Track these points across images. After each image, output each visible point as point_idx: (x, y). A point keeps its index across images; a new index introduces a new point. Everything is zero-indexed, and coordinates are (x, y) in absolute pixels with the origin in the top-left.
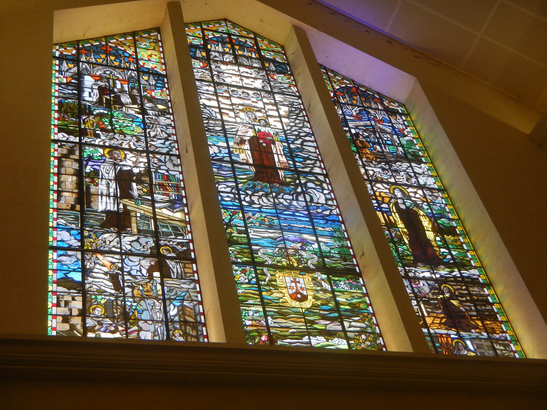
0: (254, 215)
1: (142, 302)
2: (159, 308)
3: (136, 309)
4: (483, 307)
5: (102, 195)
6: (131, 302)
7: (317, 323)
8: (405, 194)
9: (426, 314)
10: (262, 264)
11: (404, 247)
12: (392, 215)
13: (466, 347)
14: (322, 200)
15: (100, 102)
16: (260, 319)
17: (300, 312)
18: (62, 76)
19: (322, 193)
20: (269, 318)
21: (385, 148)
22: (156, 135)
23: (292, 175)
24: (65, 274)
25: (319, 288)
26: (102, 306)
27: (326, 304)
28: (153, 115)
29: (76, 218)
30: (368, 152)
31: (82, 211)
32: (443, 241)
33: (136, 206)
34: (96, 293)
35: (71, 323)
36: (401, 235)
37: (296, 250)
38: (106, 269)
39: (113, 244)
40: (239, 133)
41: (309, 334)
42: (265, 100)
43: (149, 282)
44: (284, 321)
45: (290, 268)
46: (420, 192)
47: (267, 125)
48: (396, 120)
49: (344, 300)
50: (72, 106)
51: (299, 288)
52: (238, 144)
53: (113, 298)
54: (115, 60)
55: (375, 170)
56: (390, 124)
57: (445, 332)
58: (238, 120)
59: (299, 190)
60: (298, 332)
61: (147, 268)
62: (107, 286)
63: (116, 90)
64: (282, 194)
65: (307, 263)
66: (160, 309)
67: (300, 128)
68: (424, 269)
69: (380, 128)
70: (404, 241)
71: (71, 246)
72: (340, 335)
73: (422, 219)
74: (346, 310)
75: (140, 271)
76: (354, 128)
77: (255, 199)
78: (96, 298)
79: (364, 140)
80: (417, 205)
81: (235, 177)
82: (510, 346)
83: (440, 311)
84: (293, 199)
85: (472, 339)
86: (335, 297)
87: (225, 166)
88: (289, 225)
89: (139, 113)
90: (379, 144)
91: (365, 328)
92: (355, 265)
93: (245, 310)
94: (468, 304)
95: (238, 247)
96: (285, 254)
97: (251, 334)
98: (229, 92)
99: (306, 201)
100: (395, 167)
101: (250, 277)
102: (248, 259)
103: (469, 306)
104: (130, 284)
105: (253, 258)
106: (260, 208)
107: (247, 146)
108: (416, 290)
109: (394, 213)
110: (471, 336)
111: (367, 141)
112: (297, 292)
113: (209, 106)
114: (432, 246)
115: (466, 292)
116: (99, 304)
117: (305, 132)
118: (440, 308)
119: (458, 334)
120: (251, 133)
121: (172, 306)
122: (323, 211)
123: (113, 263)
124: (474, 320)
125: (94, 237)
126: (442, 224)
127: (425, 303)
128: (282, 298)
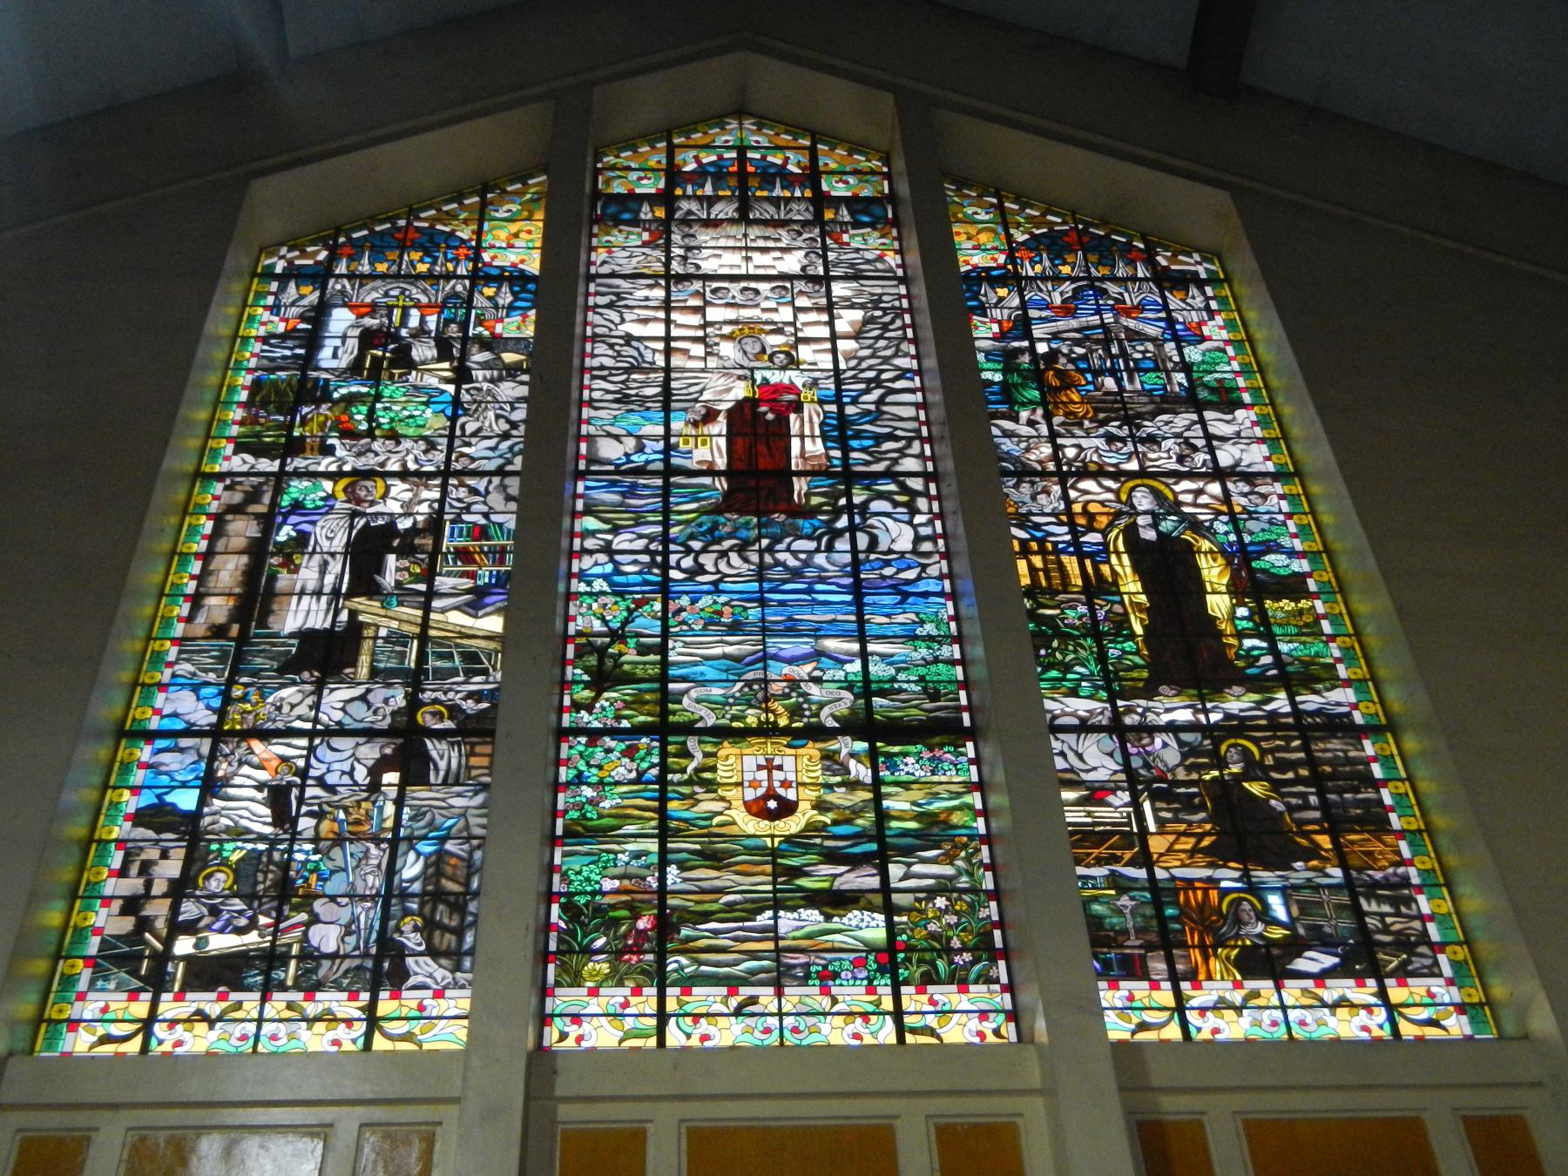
0: (694, 602)
1: (336, 853)
2: (376, 862)
3: (316, 870)
4: (1348, 796)
5: (302, 593)
6: (307, 853)
7: (808, 874)
8: (1166, 498)
9: (1152, 827)
10: (689, 729)
11: (1129, 645)
12: (1108, 562)
13: (1265, 915)
14: (905, 543)
15: (355, 369)
16: (644, 872)
17: (766, 848)
18: (276, 319)
19: (910, 523)
20: (672, 870)
21: (1131, 380)
22: (480, 429)
23: (829, 486)
24: (159, 797)
25: (838, 779)
26: (230, 867)
27: (848, 821)
28: (485, 379)
29: (221, 659)
30: (1075, 397)
31: (243, 639)
32: (1257, 618)
33: (382, 612)
34: (225, 836)
35: (144, 913)
36: (1126, 614)
37: (794, 683)
38: (263, 776)
39: (298, 711)
40: (706, 396)
41: (777, 905)
42: (802, 302)
43: (366, 799)
44: (713, 873)
45: (766, 731)
46: (1215, 488)
47: (792, 362)
48: (1183, 301)
49: (907, 806)
50: (283, 386)
51: (776, 784)
52: (695, 424)
53: (262, 847)
54: (421, 261)
55: (1085, 443)
56: (1163, 315)
57: (1207, 873)
58: (712, 363)
59: (843, 522)
60: (746, 901)
61: (370, 763)
62: (255, 815)
63: (404, 332)
64: (788, 540)
65: (817, 715)
66: (379, 866)
67: (886, 360)
68: (1176, 702)
69: (1127, 329)
70: (1130, 628)
71: (194, 724)
72: (870, 903)
73: (1203, 562)
74: (905, 833)
75: (351, 773)
76: (1048, 341)
77: (707, 561)
78: (220, 851)
79: (1070, 366)
80: (1195, 525)
81: (666, 511)
82: (1416, 901)
83: (1202, 815)
84: (818, 550)
85: (1286, 892)
86: (878, 798)
87: (645, 486)
88: (790, 619)
89: (447, 381)
90: (1113, 372)
91: (950, 878)
92: (960, 709)
93: (608, 852)
94: (1301, 789)
95: (629, 690)
96: (760, 695)
97: (611, 914)
98: (704, 295)
99: (854, 550)
100: (1149, 428)
101: (645, 765)
102: (650, 719)
103: (1304, 796)
104: (316, 808)
105: (665, 713)
106: (715, 583)
107: (720, 426)
108: (1136, 762)
109: (1118, 554)
110: (1287, 879)
111: (1078, 370)
112: (771, 794)
113: (640, 339)
114: (1221, 634)
115: (1302, 755)
116: (225, 862)
117: (898, 368)
118: (1203, 807)
119: (1245, 876)
120: (741, 391)
121: (412, 856)
122: (899, 571)
123: (284, 759)
124: (1306, 835)
125: (254, 698)
126: (1264, 571)
127: (1155, 796)
128: (721, 813)
